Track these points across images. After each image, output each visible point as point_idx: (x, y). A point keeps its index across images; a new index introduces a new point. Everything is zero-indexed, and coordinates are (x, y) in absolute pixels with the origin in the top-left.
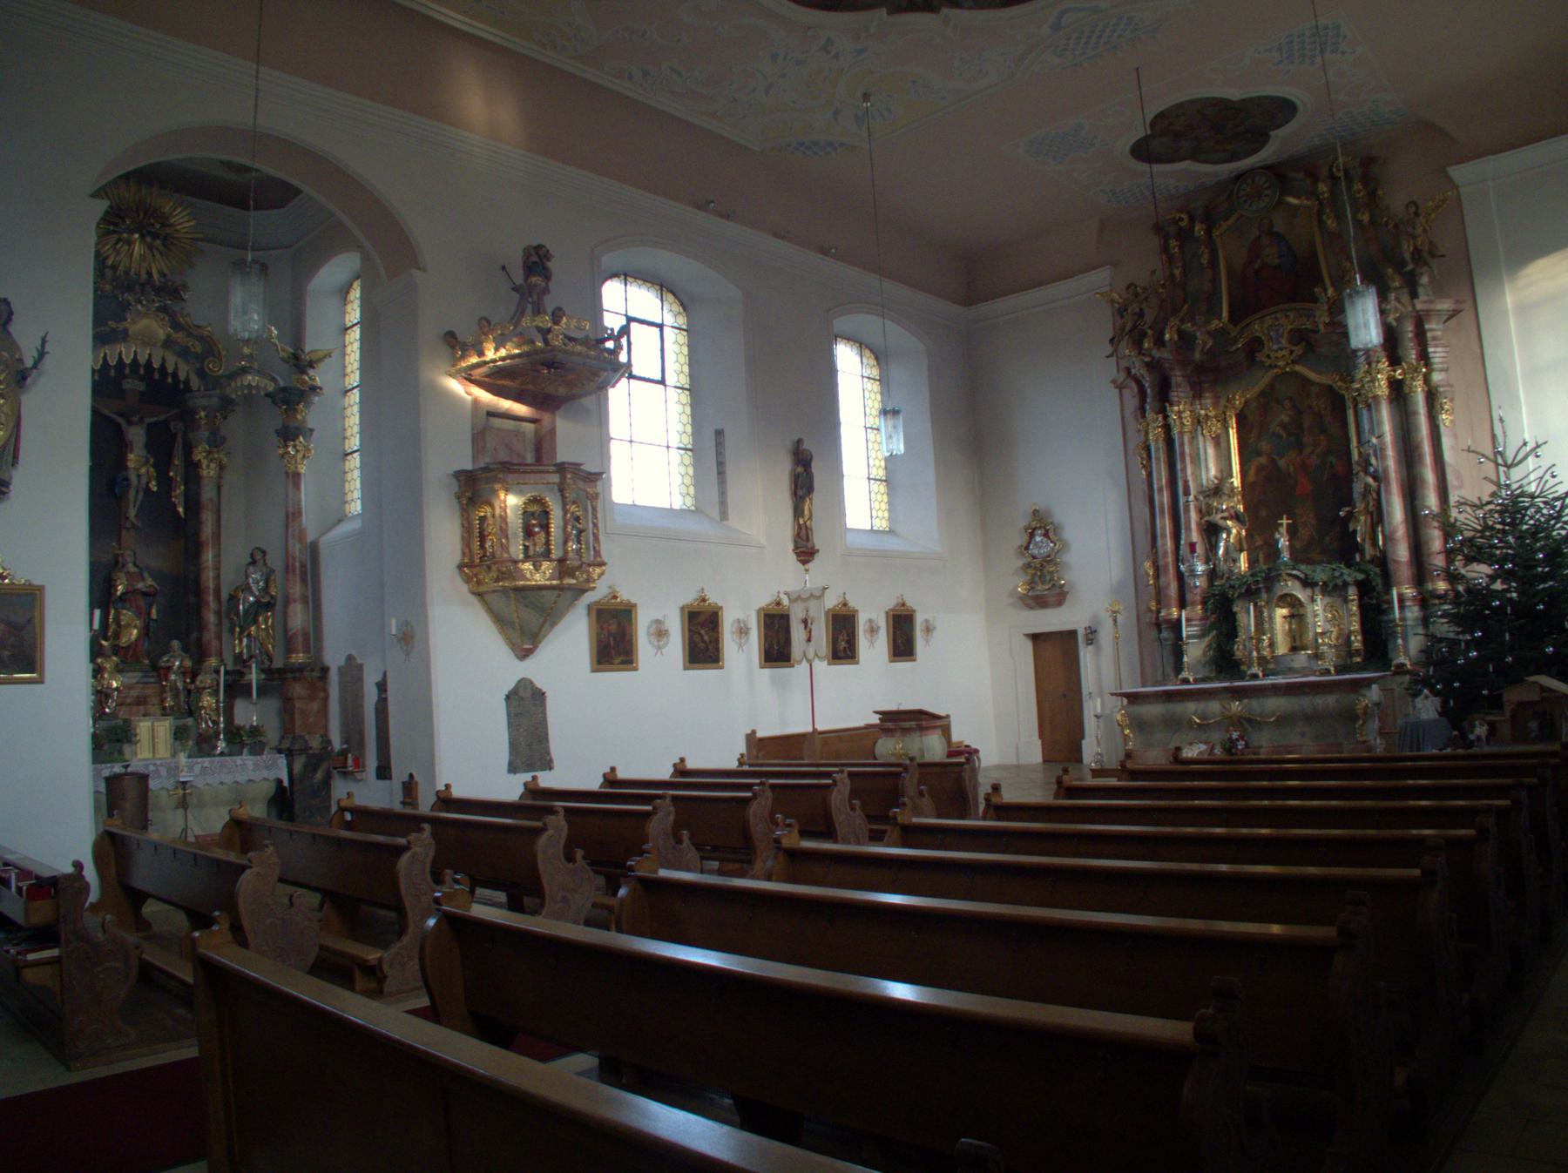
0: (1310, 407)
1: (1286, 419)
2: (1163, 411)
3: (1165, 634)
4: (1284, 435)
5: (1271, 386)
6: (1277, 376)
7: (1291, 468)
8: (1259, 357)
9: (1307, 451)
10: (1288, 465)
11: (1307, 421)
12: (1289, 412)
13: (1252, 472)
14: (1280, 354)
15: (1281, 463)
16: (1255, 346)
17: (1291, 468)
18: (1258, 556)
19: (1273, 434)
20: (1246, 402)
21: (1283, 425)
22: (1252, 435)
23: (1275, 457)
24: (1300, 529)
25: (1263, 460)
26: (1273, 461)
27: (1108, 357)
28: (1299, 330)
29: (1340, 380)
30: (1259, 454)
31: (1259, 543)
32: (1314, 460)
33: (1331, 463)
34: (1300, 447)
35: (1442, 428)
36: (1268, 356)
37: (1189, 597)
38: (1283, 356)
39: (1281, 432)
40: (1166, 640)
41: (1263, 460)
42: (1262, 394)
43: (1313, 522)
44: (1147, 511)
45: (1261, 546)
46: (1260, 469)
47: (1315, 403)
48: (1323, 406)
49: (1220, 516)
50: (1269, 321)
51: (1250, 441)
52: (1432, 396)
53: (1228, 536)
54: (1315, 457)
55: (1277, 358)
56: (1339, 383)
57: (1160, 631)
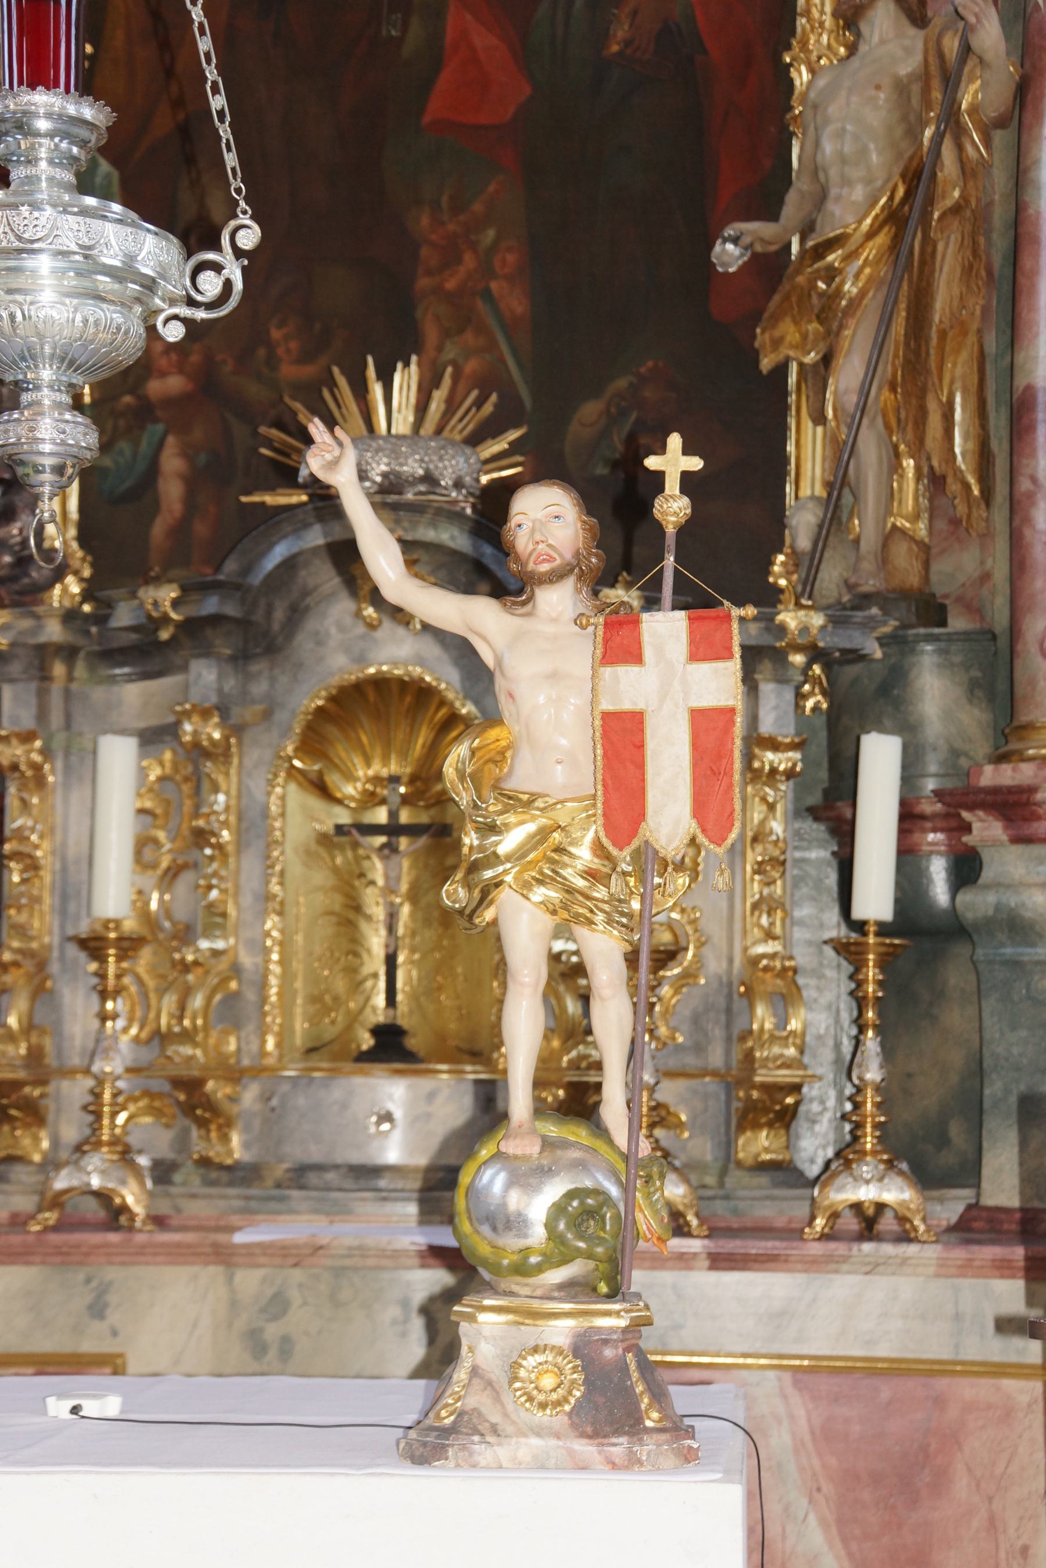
18: (153, 470)
45: (170, 402)
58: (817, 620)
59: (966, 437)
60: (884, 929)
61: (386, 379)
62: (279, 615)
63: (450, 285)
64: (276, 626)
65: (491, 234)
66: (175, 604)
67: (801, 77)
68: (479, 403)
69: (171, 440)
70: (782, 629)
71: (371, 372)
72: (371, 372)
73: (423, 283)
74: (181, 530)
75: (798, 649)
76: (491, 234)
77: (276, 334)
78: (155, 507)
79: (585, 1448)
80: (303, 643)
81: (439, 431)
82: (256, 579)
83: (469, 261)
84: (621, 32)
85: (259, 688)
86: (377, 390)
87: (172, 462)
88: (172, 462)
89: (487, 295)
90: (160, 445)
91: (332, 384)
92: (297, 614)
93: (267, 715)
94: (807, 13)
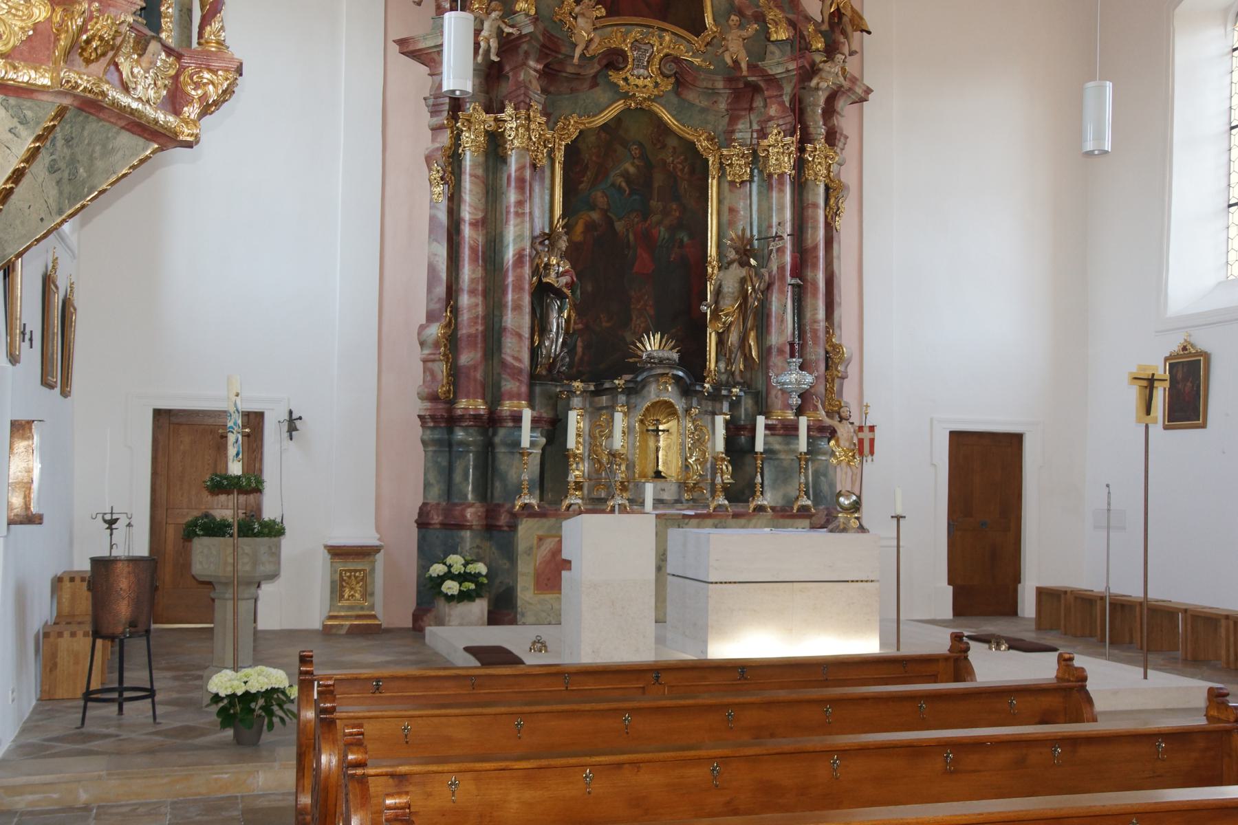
0: (664, 162)
1: (632, 170)
2: (493, 107)
3: (460, 435)
4: (627, 192)
5: (618, 119)
6: (628, 110)
7: (631, 237)
8: (616, 78)
9: (655, 219)
10: (627, 230)
11: (659, 179)
12: (636, 161)
13: (579, 228)
14: (640, 82)
15: (619, 226)
16: (614, 60)
17: (631, 237)
18: (575, 346)
19: (613, 185)
20: (581, 132)
21: (626, 175)
22: (585, 179)
23: (614, 217)
24: (634, 318)
25: (595, 216)
26: (610, 223)
27: (414, 2)
28: (677, 60)
29: (708, 139)
30: (593, 207)
31: (580, 326)
32: (662, 232)
33: (682, 241)
34: (646, 214)
35: (835, 231)
36: (626, 80)
37: (509, 385)
38: (645, 86)
39: (624, 184)
40: (461, 443)
41: (595, 216)
42: (605, 127)
43: (652, 312)
44: (442, 250)
46: (590, 227)
47: (671, 159)
48: (680, 166)
49: (564, 280)
50: (636, 33)
51: (582, 186)
52: (827, 188)
53: (560, 310)
54: (662, 229)
55: (637, 86)
56: (705, 143)
57: (450, 431)
58: (738, 390)
59: (755, 351)
60: (761, 453)
61: (654, 336)
62: (640, 387)
63: (639, 307)
64: (638, 389)
65: (646, 297)
66: (624, 384)
67: (710, 270)
68: (671, 342)
69: (579, 339)
70: (732, 392)
71: (651, 335)
72: (651, 335)
73: (632, 306)
74: (581, 359)
75: (734, 396)
76: (646, 297)
77: (602, 316)
78: (576, 354)
79: (859, 531)
80: (645, 392)
81: (663, 348)
82: (639, 379)
83: (642, 303)
84: (673, 256)
85: (633, 401)
86: (652, 338)
87: (579, 344)
88: (579, 344)
89: (645, 309)
90: (576, 342)
91: (644, 337)
92: (643, 387)
93: (635, 406)
94: (711, 256)
